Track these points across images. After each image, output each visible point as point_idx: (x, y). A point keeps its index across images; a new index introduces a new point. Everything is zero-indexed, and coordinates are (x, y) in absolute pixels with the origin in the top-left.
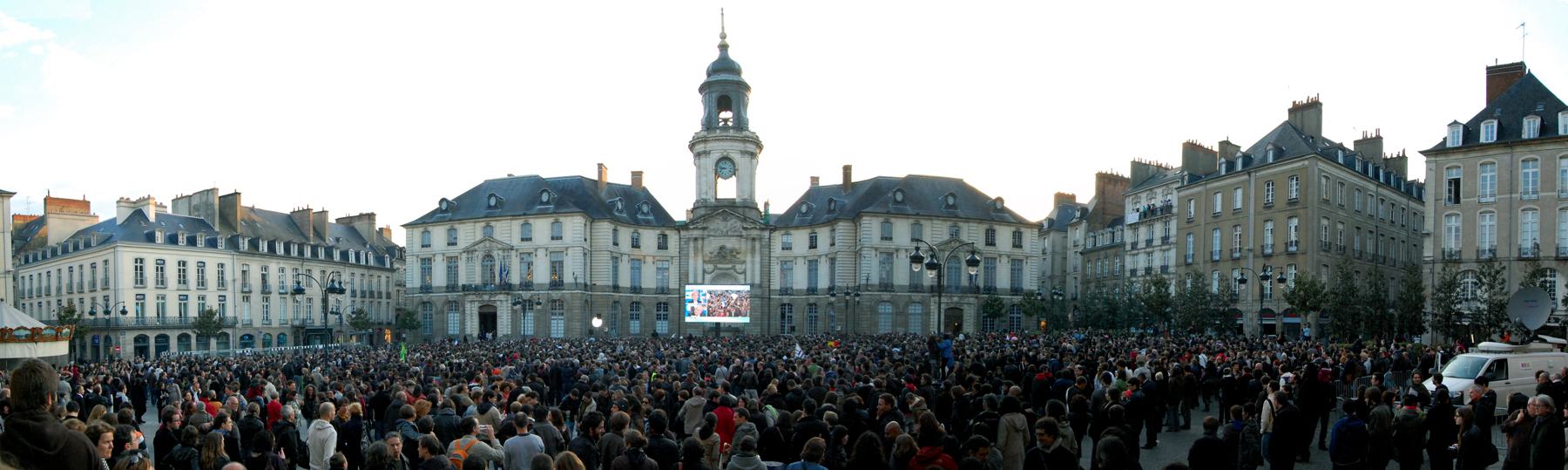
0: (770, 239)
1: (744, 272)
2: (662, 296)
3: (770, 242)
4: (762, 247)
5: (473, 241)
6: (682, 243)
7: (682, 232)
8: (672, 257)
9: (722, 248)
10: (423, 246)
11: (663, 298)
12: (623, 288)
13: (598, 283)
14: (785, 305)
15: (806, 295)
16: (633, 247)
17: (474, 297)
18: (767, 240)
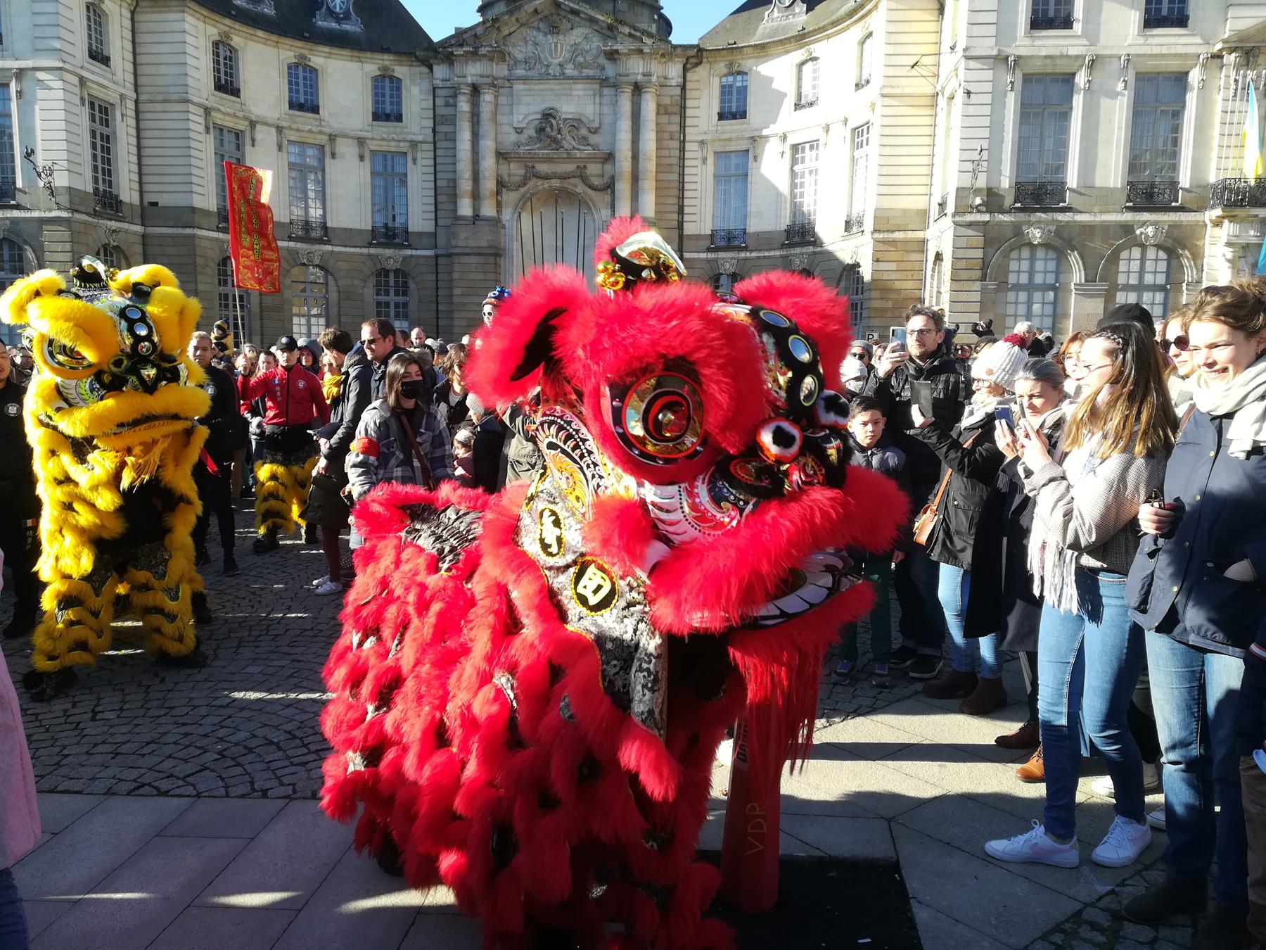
0: (683, 88)
2: (388, 252)
3: (683, 97)
4: (661, 110)
6: (439, 101)
7: (436, 68)
8: (414, 144)
9: (548, 115)
11: (391, 256)
13: (165, 200)
15: (783, 246)
16: (292, 106)
18: (678, 91)
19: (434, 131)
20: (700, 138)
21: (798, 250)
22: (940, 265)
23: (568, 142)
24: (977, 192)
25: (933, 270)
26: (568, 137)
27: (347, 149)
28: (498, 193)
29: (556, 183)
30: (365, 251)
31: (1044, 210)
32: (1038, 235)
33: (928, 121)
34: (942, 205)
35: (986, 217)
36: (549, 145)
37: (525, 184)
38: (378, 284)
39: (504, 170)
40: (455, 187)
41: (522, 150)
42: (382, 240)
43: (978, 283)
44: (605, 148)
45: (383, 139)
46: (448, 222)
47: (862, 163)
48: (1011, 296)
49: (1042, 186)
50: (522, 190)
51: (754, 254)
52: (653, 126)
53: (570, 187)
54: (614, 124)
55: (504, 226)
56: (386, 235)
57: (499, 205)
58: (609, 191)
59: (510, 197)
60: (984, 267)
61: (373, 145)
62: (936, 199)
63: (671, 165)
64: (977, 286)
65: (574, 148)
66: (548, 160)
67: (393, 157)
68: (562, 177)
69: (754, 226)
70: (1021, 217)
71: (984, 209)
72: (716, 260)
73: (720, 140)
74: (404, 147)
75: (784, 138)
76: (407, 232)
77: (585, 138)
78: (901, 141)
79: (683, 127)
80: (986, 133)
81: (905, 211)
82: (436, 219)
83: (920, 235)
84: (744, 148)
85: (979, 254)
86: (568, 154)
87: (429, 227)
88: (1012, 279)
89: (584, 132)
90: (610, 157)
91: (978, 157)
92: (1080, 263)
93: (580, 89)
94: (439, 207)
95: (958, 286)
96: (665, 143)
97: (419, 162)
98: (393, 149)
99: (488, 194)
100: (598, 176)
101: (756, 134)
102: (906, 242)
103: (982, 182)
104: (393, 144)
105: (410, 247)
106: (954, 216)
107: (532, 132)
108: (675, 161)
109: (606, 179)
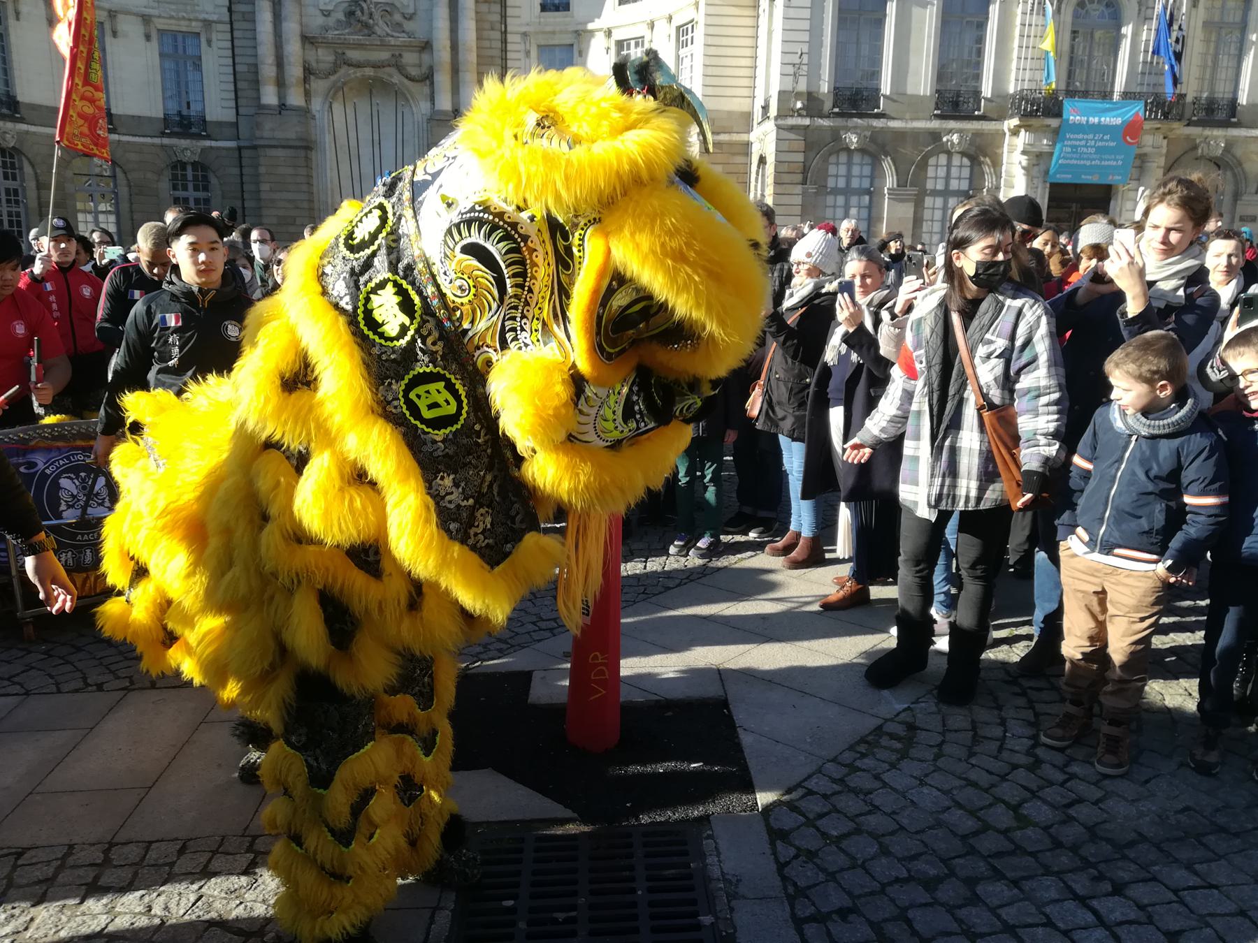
2: (184, 143)
8: (208, 24)
11: (188, 148)
12: (33, 107)
19: (230, 10)
20: (523, 29)
22: (764, 169)
23: (381, 28)
24: (798, 95)
25: (757, 173)
26: (381, 22)
27: (131, 28)
28: (306, 80)
29: (369, 72)
30: (157, 141)
31: (861, 116)
32: (855, 140)
33: (750, 22)
34: (765, 108)
35: (807, 121)
36: (360, 31)
37: (335, 72)
38: (174, 177)
39: (311, 56)
40: (257, 73)
41: (331, 34)
42: (176, 129)
43: (800, 187)
44: (421, 36)
45: (171, 17)
46: (252, 111)
47: (687, 62)
48: (830, 200)
49: (858, 92)
50: (333, 78)
52: (473, 14)
53: (385, 77)
54: (430, 11)
55: (313, 117)
56: (180, 124)
57: (307, 94)
58: (428, 82)
59: (318, 85)
60: (805, 171)
61: (160, 24)
62: (759, 102)
63: (492, 57)
64: (799, 189)
65: (388, 35)
66: (359, 46)
67: (184, 38)
68: (375, 66)
70: (839, 122)
71: (805, 113)
73: (544, 33)
74: (196, 27)
75: (609, 33)
76: (204, 121)
77: (399, 25)
78: (725, 41)
79: (504, 17)
80: (806, 37)
81: (730, 113)
82: (237, 108)
83: (744, 137)
84: (569, 42)
85: (800, 157)
86: (381, 40)
87: (229, 116)
88: (831, 183)
89: (397, 17)
90: (427, 46)
91: (798, 61)
92: (893, 168)
94: (239, 94)
95: (781, 189)
96: (486, 34)
97: (214, 44)
98: (184, 29)
99: (294, 80)
100: (414, 66)
101: (579, 27)
102: (731, 144)
103: (802, 86)
104: (183, 23)
105: (208, 137)
106: (776, 118)
107: (341, 16)
108: (497, 53)
109: (424, 70)
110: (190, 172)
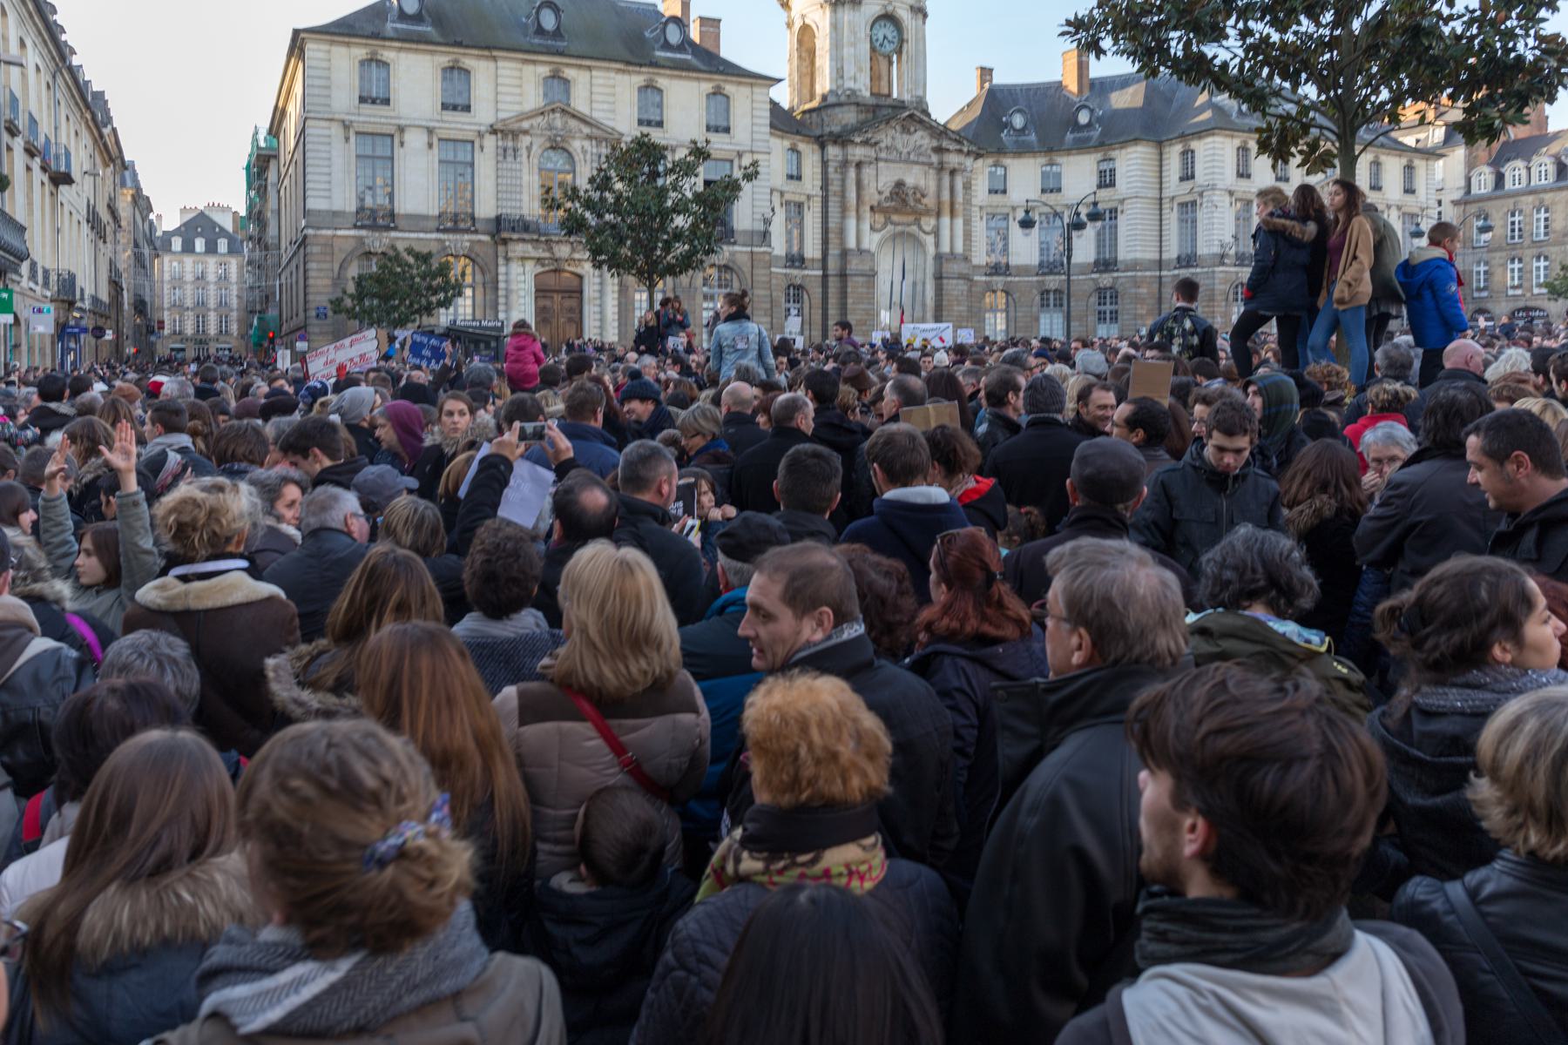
1: (936, 232)
5: (517, 108)
8: (809, 197)
9: (900, 184)
10: (362, 100)
14: (1048, 292)
15: (1037, 274)
17: (528, 249)
21: (1051, 277)
38: (1042, 299)
51: (1017, 279)
69: (1015, 260)
72: (990, 282)
93: (917, 169)
110: (1051, 296)
